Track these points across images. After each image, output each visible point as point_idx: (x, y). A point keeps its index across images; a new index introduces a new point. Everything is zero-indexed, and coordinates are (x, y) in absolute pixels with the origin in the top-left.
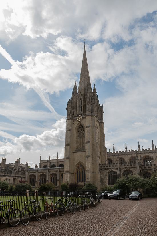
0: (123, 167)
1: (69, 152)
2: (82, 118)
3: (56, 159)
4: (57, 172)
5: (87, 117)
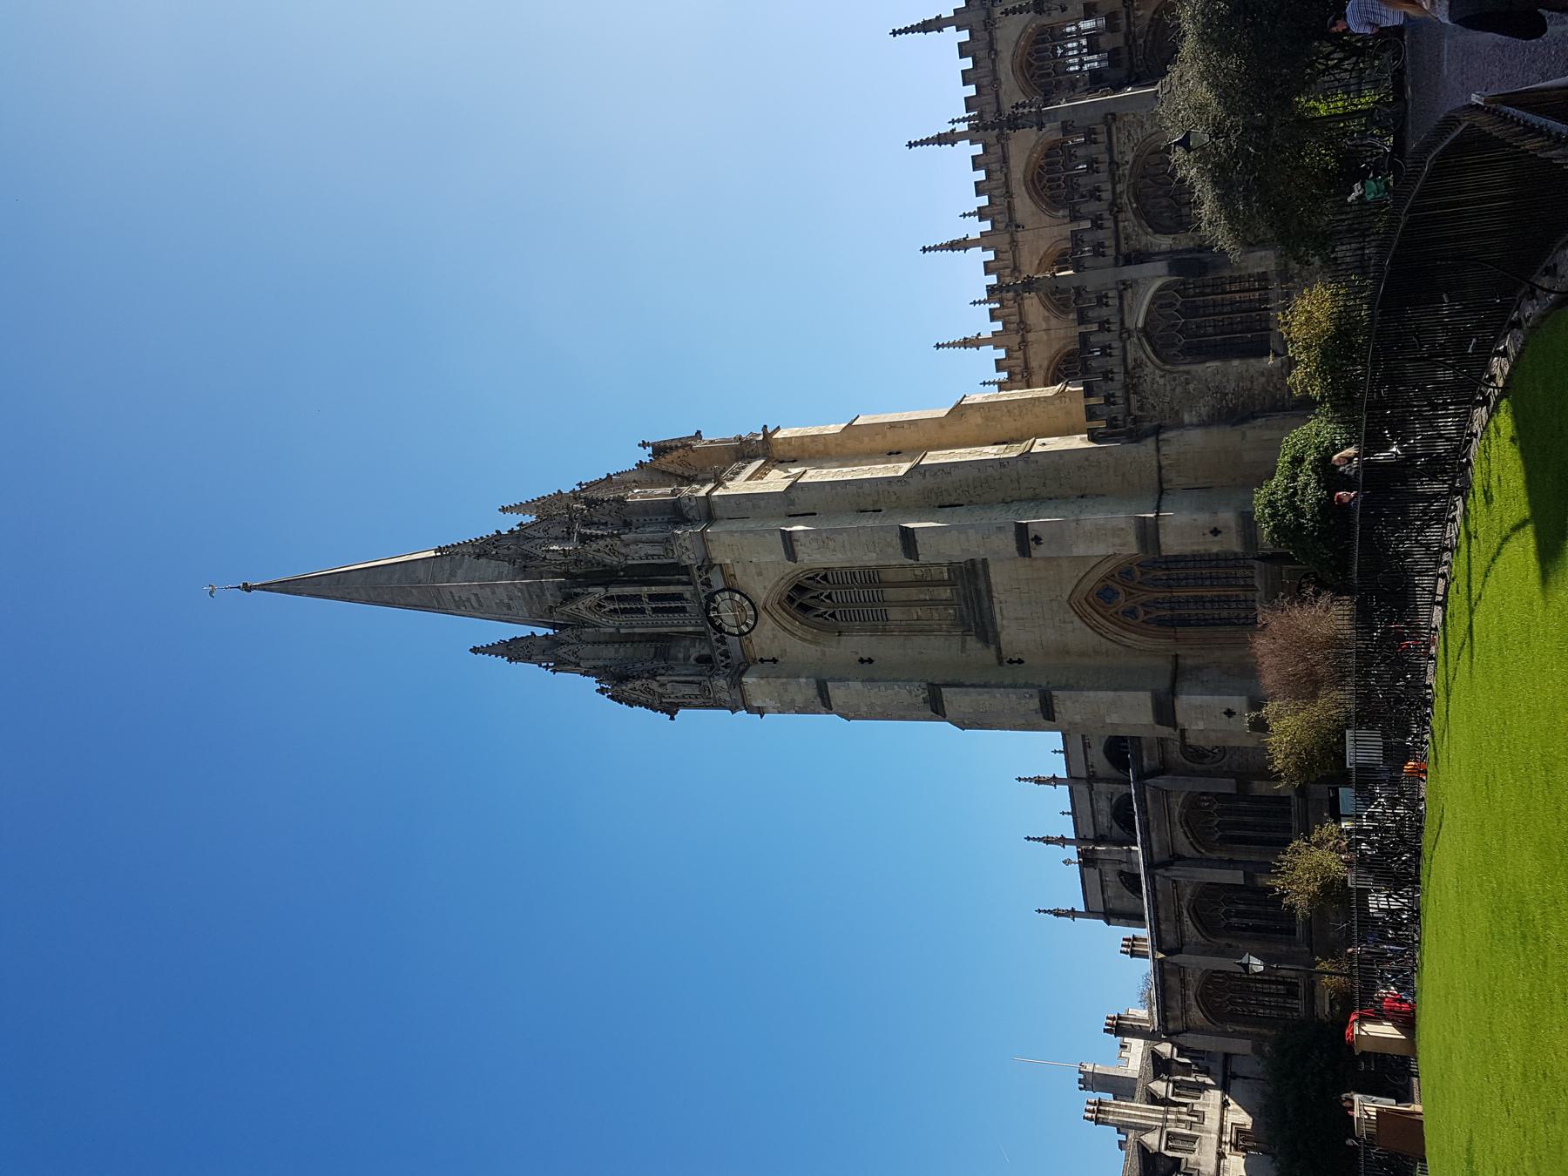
0: (1105, 235)
1: (998, 693)
2: (727, 595)
3: (1071, 791)
5: (719, 556)
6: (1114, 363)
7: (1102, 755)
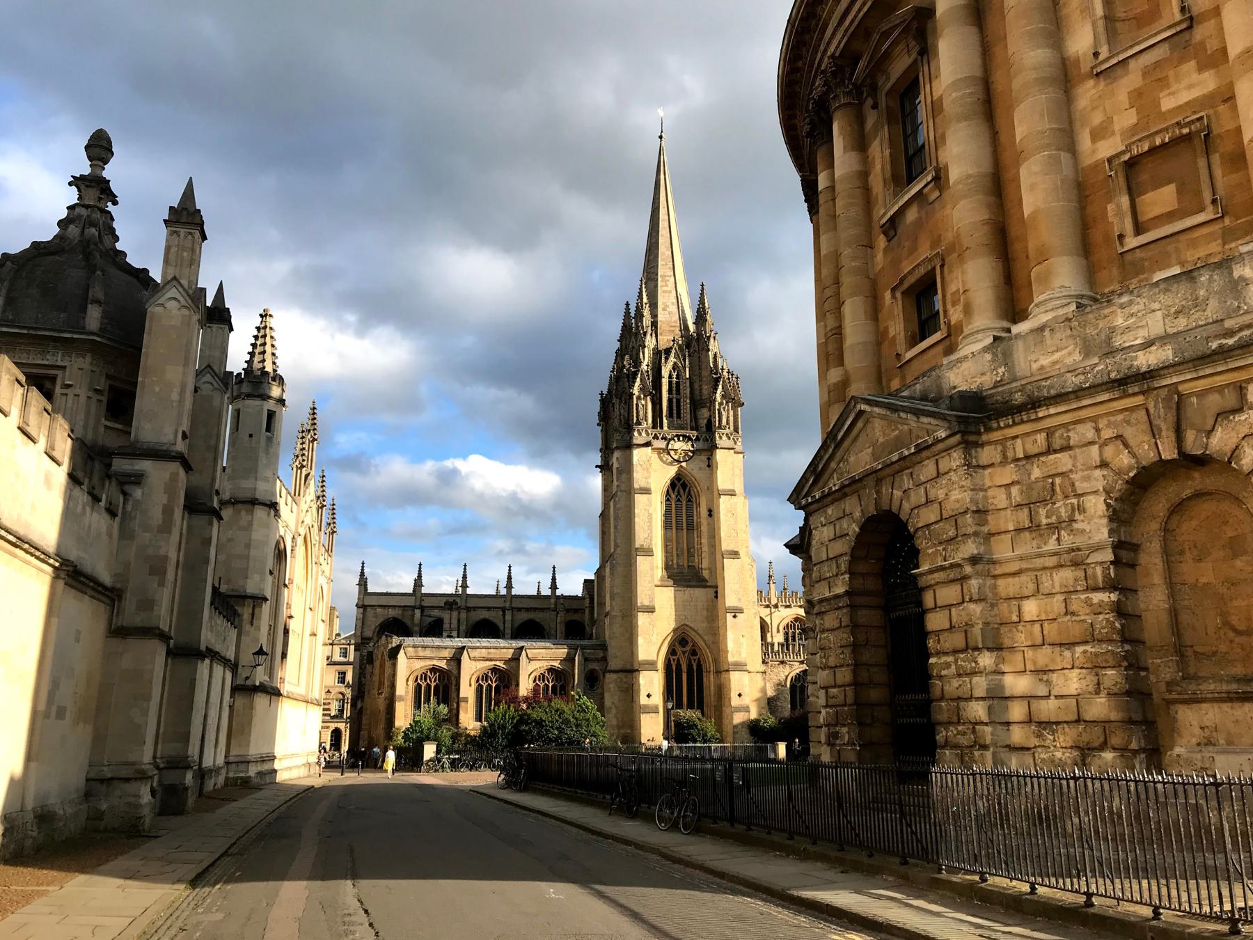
7: (482, 617)
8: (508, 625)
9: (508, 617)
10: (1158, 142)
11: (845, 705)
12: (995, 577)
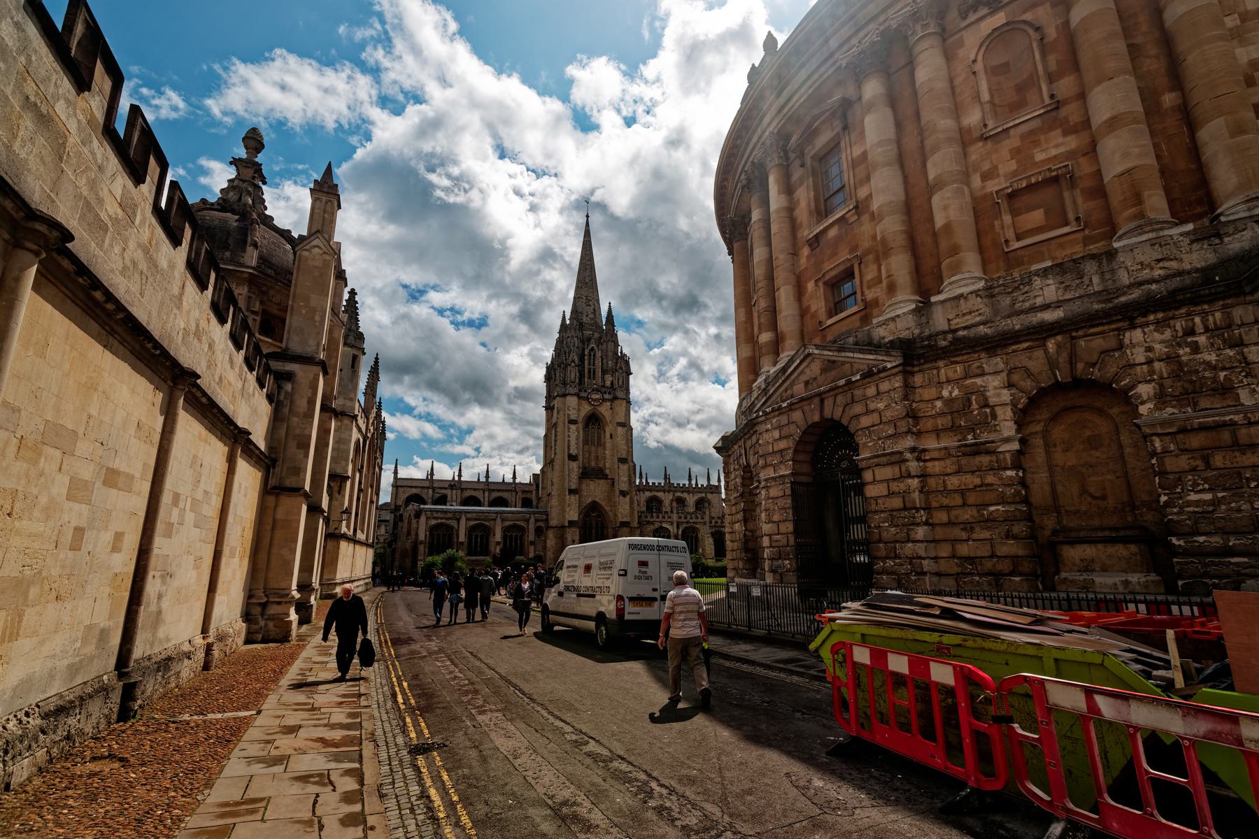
0: (683, 520)
4: (528, 521)
5: (617, 402)
6: (655, 519)
8: (486, 499)
9: (487, 494)
10: (1033, 180)
11: (788, 546)
12: (925, 461)
